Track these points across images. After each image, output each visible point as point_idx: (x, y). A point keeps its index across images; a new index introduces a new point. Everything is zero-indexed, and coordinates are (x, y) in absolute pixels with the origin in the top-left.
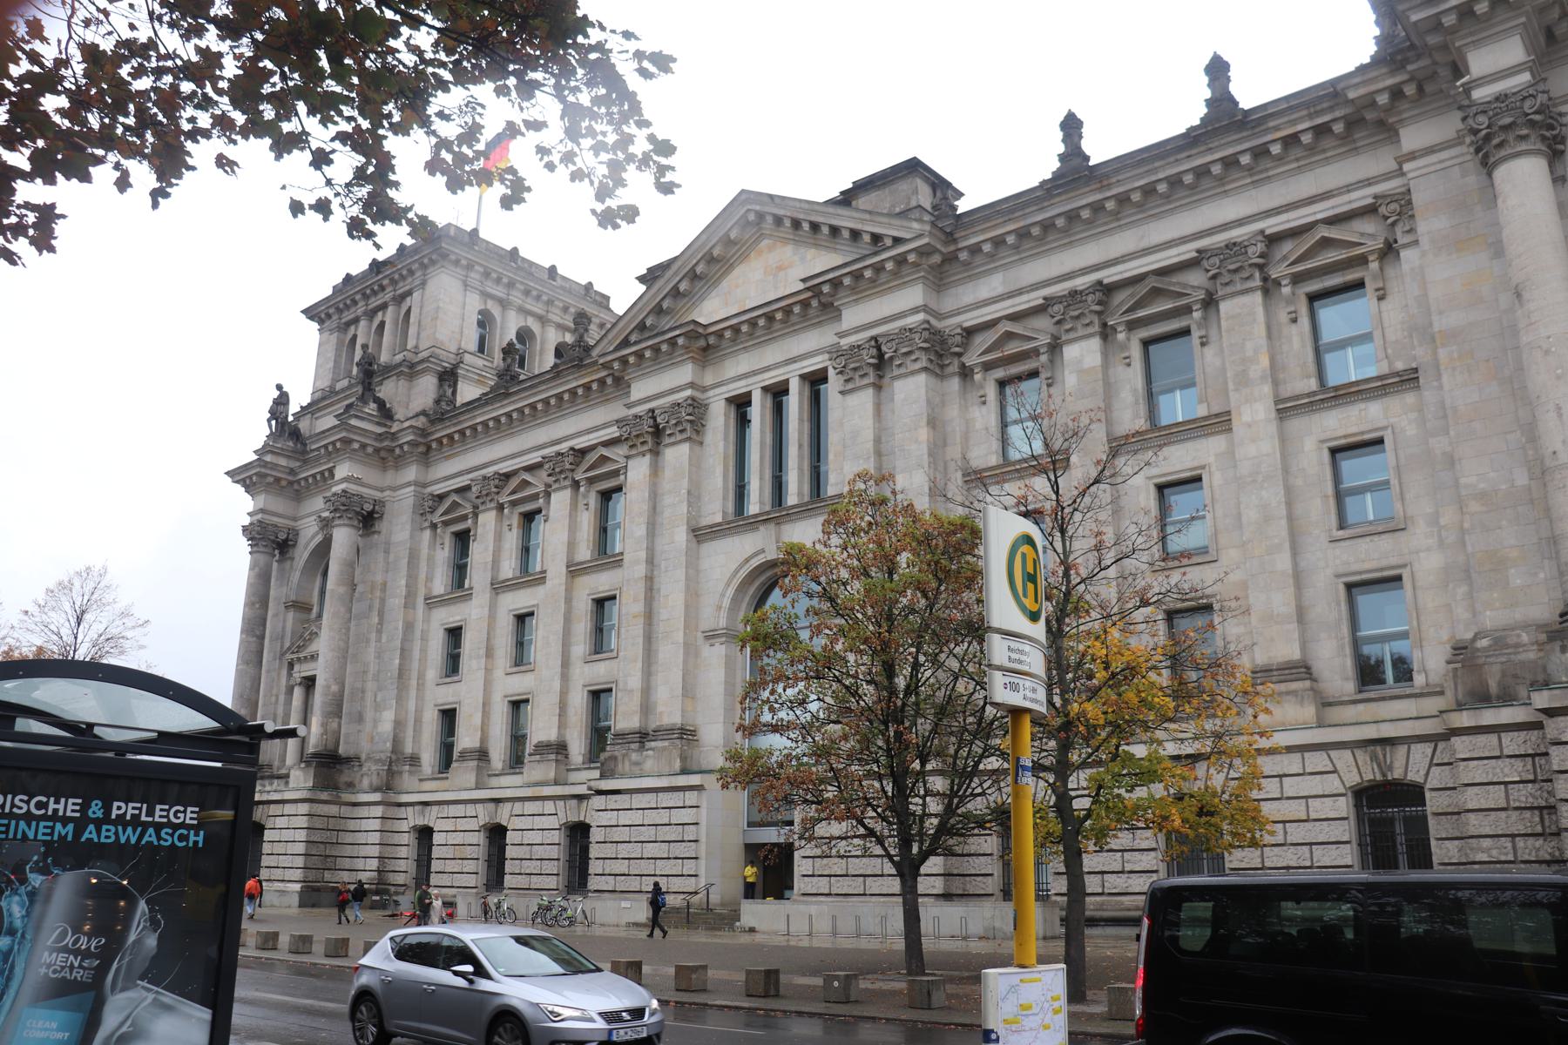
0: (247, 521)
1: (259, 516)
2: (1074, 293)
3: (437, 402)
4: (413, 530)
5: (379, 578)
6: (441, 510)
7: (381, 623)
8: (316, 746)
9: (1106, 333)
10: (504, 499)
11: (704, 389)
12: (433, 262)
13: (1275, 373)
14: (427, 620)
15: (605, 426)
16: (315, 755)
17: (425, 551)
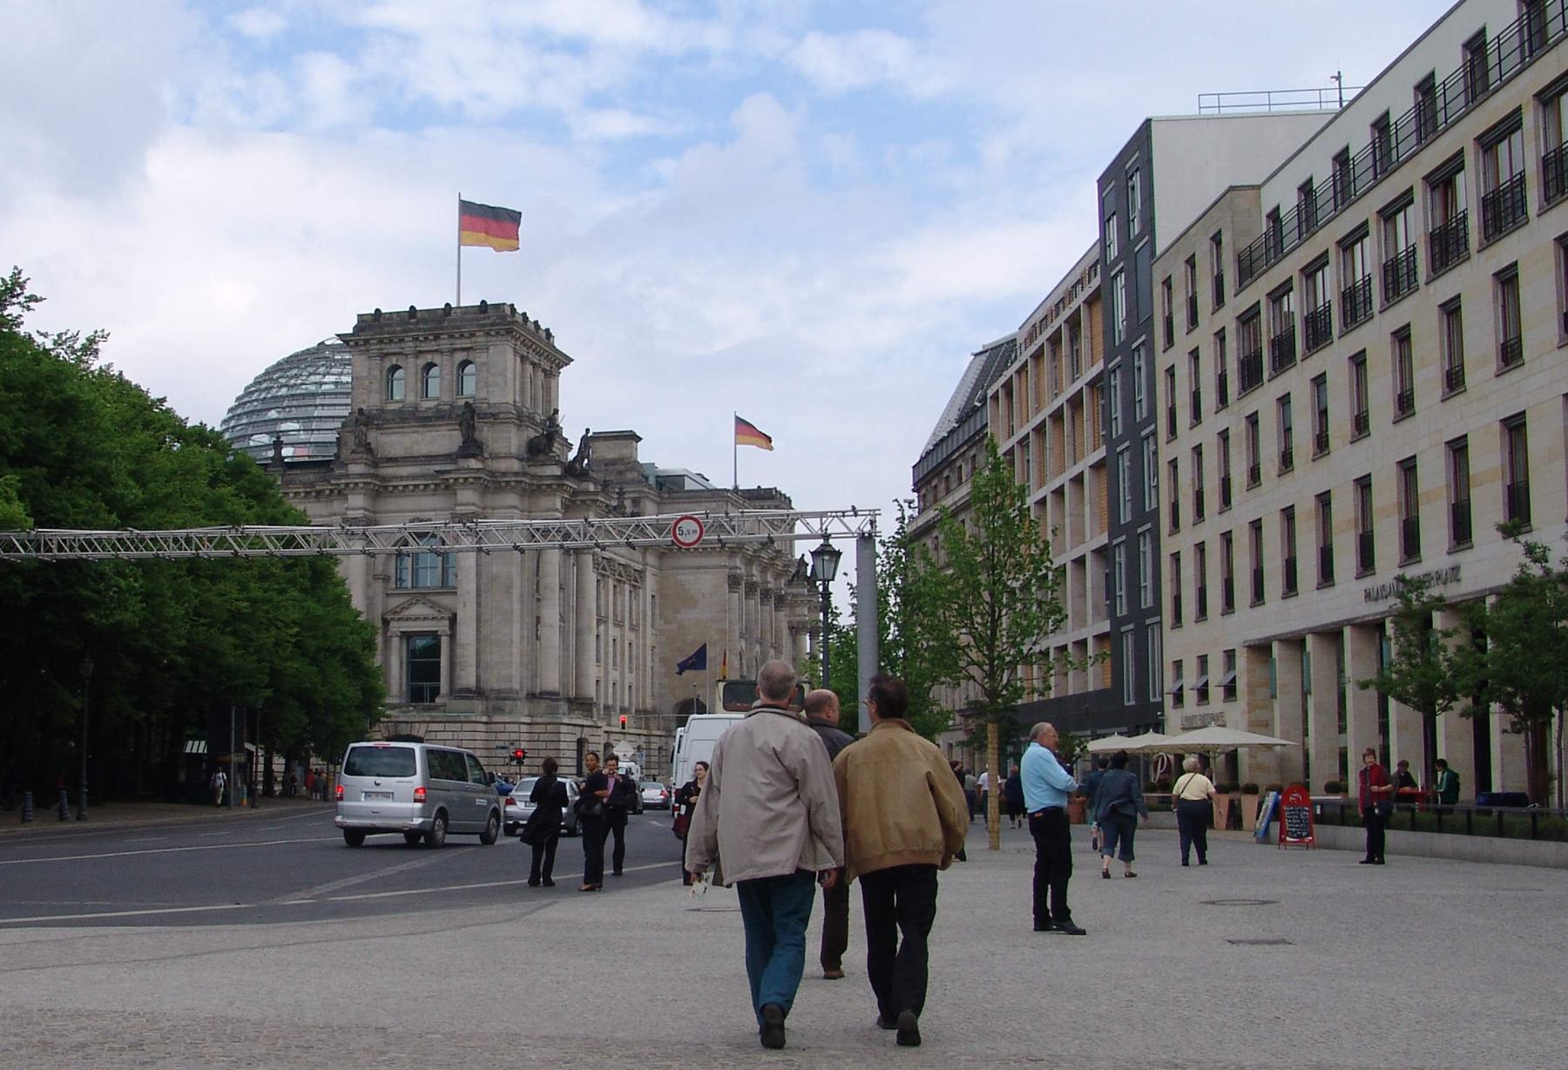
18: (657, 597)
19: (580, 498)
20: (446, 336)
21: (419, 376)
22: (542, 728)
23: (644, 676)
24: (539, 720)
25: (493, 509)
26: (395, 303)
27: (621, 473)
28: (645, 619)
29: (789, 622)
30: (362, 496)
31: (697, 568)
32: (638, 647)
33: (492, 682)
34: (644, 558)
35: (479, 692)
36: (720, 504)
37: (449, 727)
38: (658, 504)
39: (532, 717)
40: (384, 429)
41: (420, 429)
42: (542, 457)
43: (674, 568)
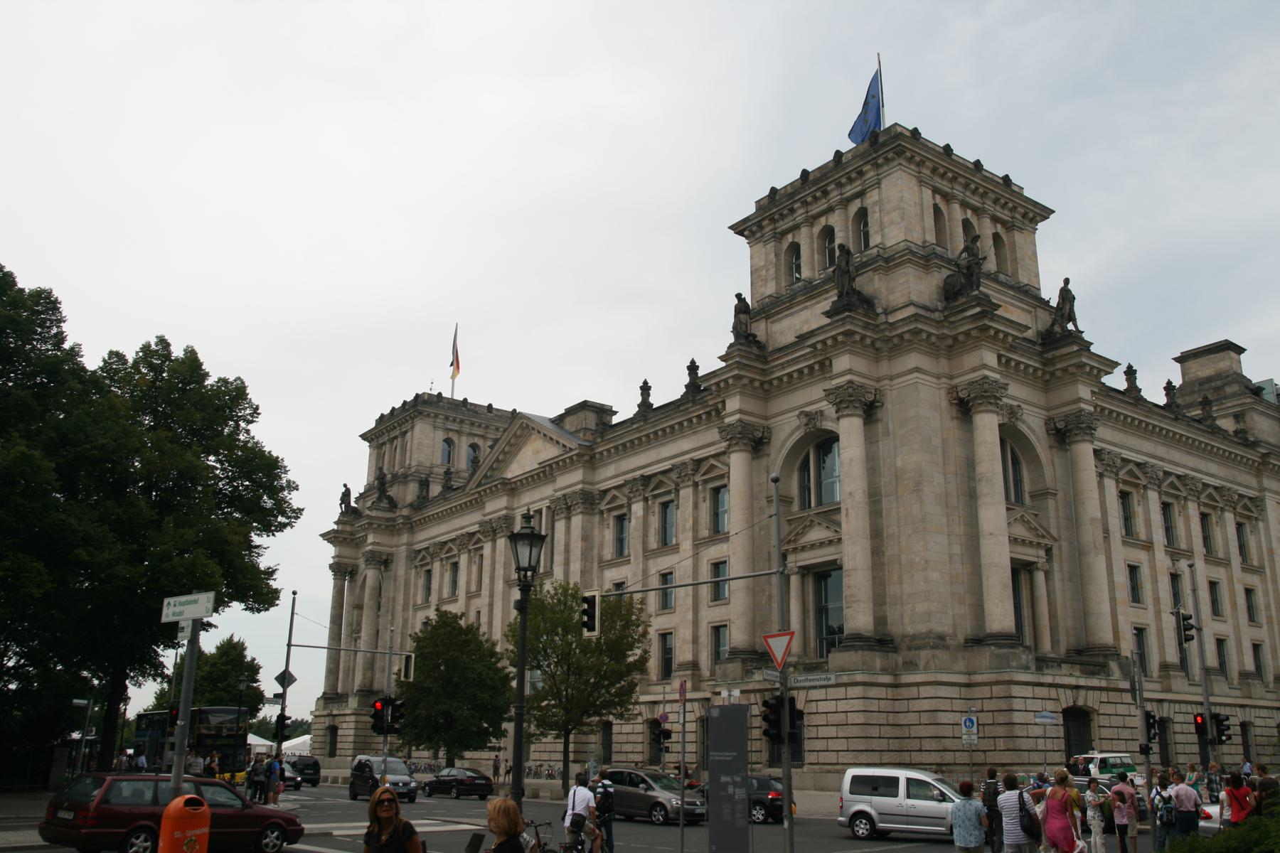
0: (331, 561)
1: (336, 559)
2: (635, 479)
3: (418, 497)
4: (406, 569)
5: (391, 595)
6: (419, 559)
7: (393, 619)
8: (359, 686)
9: (646, 500)
10: (443, 556)
11: (513, 509)
12: (416, 417)
13: (695, 529)
14: (414, 617)
15: (474, 524)
16: (358, 691)
17: (413, 581)
19: (1058, 366)
20: (832, 186)
21: (816, 246)
22: (985, 691)
24: (978, 678)
25: (891, 378)
26: (786, 176)
27: (1217, 389)
30: (738, 397)
32: (1266, 594)
33: (906, 622)
34: (1260, 482)
35: (882, 642)
37: (833, 693)
40: (774, 315)
41: (808, 304)
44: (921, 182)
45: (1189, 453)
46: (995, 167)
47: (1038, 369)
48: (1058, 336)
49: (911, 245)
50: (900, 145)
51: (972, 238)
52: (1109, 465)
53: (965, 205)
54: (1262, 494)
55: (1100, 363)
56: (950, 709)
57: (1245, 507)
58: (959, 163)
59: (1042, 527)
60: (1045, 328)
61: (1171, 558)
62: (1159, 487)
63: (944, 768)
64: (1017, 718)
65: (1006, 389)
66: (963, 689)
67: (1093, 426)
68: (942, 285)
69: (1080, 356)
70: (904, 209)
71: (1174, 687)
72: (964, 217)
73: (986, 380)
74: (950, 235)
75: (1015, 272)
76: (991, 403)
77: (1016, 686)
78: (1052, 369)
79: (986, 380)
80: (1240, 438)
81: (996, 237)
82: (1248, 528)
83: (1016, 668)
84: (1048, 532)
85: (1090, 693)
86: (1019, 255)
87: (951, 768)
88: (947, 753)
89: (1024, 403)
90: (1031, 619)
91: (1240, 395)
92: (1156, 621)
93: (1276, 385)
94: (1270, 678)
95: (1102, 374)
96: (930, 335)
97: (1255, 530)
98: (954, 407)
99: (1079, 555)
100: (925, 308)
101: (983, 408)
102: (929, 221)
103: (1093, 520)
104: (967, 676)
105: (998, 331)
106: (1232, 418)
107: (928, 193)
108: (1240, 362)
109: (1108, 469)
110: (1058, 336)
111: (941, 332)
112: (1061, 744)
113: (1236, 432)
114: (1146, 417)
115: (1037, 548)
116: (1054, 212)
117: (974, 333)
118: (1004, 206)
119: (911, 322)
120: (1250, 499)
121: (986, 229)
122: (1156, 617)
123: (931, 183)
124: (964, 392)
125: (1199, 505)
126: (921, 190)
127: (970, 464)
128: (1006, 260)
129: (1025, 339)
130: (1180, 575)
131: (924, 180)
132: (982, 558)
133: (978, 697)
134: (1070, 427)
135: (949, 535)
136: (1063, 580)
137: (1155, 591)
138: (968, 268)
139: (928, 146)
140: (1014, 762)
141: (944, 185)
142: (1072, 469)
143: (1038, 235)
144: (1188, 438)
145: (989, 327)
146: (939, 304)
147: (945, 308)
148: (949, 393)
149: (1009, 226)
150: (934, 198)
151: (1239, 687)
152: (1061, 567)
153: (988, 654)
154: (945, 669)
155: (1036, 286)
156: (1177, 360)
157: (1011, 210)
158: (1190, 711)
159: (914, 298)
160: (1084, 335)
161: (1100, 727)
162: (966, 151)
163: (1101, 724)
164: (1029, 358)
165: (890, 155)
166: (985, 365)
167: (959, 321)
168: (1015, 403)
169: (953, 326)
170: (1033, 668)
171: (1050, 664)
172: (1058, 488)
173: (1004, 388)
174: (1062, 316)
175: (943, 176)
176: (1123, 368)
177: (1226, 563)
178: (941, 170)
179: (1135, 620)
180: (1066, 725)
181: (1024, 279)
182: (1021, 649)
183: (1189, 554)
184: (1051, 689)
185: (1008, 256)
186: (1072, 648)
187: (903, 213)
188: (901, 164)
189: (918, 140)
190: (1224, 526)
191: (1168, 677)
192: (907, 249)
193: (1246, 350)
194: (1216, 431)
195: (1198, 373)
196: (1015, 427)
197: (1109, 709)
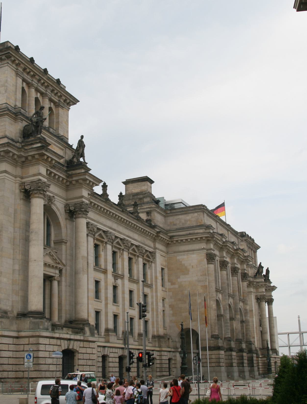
18: (166, 270)
19: (74, 179)
22: (26, 341)
23: (157, 315)
24: (23, 334)
27: (140, 199)
28: (156, 281)
29: (256, 296)
31: (188, 251)
32: (152, 297)
34: (155, 245)
36: (199, 213)
38: (165, 217)
39: (18, 331)
42: (32, 139)
43: (175, 252)
44: (17, 74)
45: (126, 228)
46: (54, 74)
47: (65, 179)
48: (75, 163)
49: (9, 106)
50: (9, 53)
51: (40, 109)
52: (91, 231)
53: (37, 90)
54: (155, 250)
55: (94, 179)
56: (7, 349)
57: (148, 256)
58: (37, 68)
59: (59, 258)
60: (69, 159)
61: (114, 278)
62: (112, 243)
63: (2, 380)
64: (41, 354)
65: (49, 187)
66: (14, 339)
67: (88, 210)
68: (22, 129)
69: (85, 175)
70: (7, 86)
71: (111, 341)
72: (36, 96)
73: (40, 181)
74: (29, 104)
75: (57, 129)
76: (41, 193)
77: (42, 338)
78: (70, 180)
79: (40, 181)
80: (148, 223)
81: (50, 109)
82: (147, 266)
83: (42, 329)
84: (61, 262)
85: (76, 342)
86: (60, 120)
87: (6, 380)
88: (4, 372)
89: (56, 195)
90: (49, 305)
91: (150, 203)
92: (105, 308)
93: (165, 200)
94: (150, 336)
95: (94, 185)
96: (14, 154)
97: (150, 267)
98: (22, 194)
99: (75, 274)
100: (12, 140)
101: (37, 195)
102: (19, 95)
103: (83, 257)
104: (17, 333)
105: (48, 157)
106: (145, 213)
107: (20, 81)
108: (151, 187)
109: (91, 232)
110: (75, 163)
111: (20, 154)
112: (60, 368)
113: (147, 220)
114: (110, 208)
115: (55, 269)
116: (79, 101)
117: (37, 156)
118: (56, 94)
119: (5, 146)
120: (150, 252)
121: (46, 104)
122: (105, 306)
123: (22, 75)
124: (28, 186)
125: (128, 254)
126: (17, 78)
127: (27, 224)
128: (54, 122)
129: (59, 163)
130: (117, 286)
131: (19, 73)
132: (29, 272)
133: (21, 343)
134: (77, 210)
135: (13, 259)
136: (66, 286)
137: (106, 293)
138: (37, 123)
139: (22, 56)
140: (38, 377)
141: (28, 78)
142: (75, 231)
143: (70, 112)
144: (127, 221)
145: (45, 154)
146: (20, 139)
147: (23, 142)
148: (20, 186)
149: (57, 105)
150: (23, 84)
151: (138, 340)
152: (66, 280)
153: (29, 322)
154: (6, 329)
155: (67, 137)
156: (124, 183)
157: (59, 97)
158: (116, 351)
159: (8, 134)
160: (87, 165)
161: (78, 359)
162: (41, 63)
163: (79, 358)
164: (61, 173)
165: (3, 57)
166: (40, 173)
167: (30, 149)
168: (52, 195)
169: (25, 151)
170: (50, 329)
171: (58, 328)
172: (68, 240)
173: (48, 187)
174: (78, 154)
175: (28, 73)
176: (102, 184)
177: (136, 282)
178: (28, 70)
179: (96, 307)
180: (63, 358)
181: (61, 133)
182: (45, 319)
183: (122, 277)
184: (58, 340)
185: (55, 120)
186: (68, 320)
187: (7, 89)
188: (8, 63)
189: (18, 52)
190: (138, 264)
191: (108, 335)
192: (7, 108)
193: (154, 182)
194: (139, 219)
195: (133, 190)
196: (50, 207)
197: (83, 351)
